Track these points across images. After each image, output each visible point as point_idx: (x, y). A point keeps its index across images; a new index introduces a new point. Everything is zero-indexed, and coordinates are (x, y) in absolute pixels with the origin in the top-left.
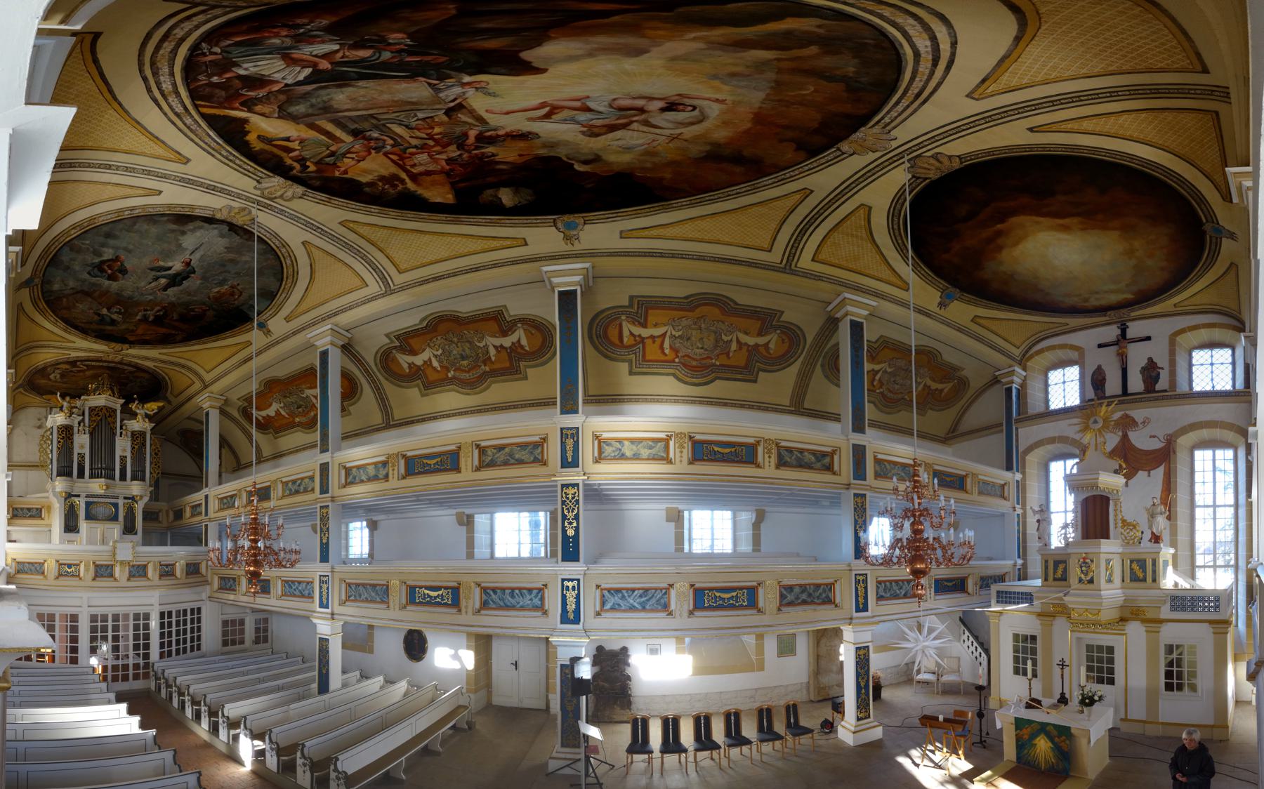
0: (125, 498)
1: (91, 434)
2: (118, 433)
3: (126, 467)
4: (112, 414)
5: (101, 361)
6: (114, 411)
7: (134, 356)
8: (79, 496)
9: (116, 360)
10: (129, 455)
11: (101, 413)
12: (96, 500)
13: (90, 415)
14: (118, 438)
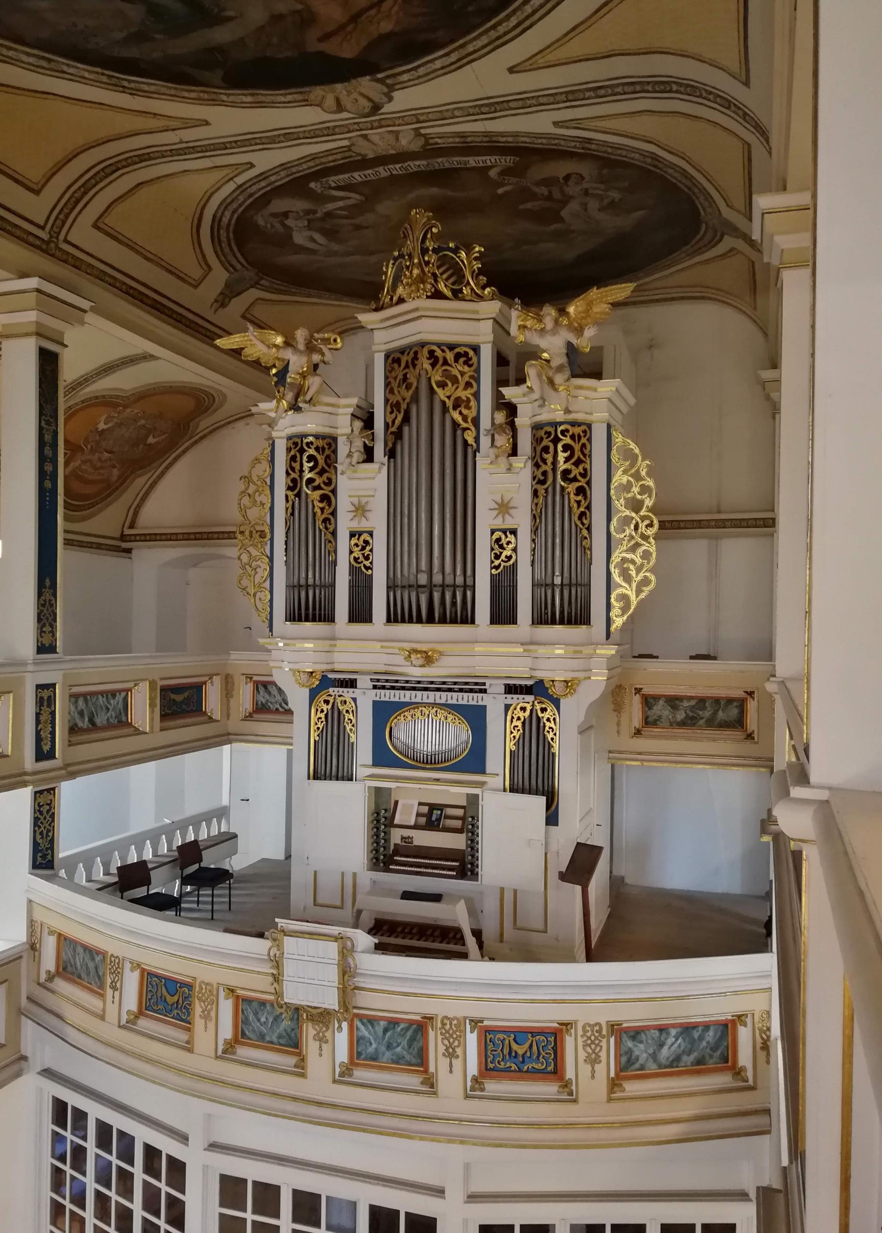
0: (510, 689)
1: (391, 454)
2: (485, 441)
5: (364, 163)
7: (446, 113)
8: (351, 684)
10: (522, 520)
12: (406, 696)
13: (387, 384)
14: (482, 462)
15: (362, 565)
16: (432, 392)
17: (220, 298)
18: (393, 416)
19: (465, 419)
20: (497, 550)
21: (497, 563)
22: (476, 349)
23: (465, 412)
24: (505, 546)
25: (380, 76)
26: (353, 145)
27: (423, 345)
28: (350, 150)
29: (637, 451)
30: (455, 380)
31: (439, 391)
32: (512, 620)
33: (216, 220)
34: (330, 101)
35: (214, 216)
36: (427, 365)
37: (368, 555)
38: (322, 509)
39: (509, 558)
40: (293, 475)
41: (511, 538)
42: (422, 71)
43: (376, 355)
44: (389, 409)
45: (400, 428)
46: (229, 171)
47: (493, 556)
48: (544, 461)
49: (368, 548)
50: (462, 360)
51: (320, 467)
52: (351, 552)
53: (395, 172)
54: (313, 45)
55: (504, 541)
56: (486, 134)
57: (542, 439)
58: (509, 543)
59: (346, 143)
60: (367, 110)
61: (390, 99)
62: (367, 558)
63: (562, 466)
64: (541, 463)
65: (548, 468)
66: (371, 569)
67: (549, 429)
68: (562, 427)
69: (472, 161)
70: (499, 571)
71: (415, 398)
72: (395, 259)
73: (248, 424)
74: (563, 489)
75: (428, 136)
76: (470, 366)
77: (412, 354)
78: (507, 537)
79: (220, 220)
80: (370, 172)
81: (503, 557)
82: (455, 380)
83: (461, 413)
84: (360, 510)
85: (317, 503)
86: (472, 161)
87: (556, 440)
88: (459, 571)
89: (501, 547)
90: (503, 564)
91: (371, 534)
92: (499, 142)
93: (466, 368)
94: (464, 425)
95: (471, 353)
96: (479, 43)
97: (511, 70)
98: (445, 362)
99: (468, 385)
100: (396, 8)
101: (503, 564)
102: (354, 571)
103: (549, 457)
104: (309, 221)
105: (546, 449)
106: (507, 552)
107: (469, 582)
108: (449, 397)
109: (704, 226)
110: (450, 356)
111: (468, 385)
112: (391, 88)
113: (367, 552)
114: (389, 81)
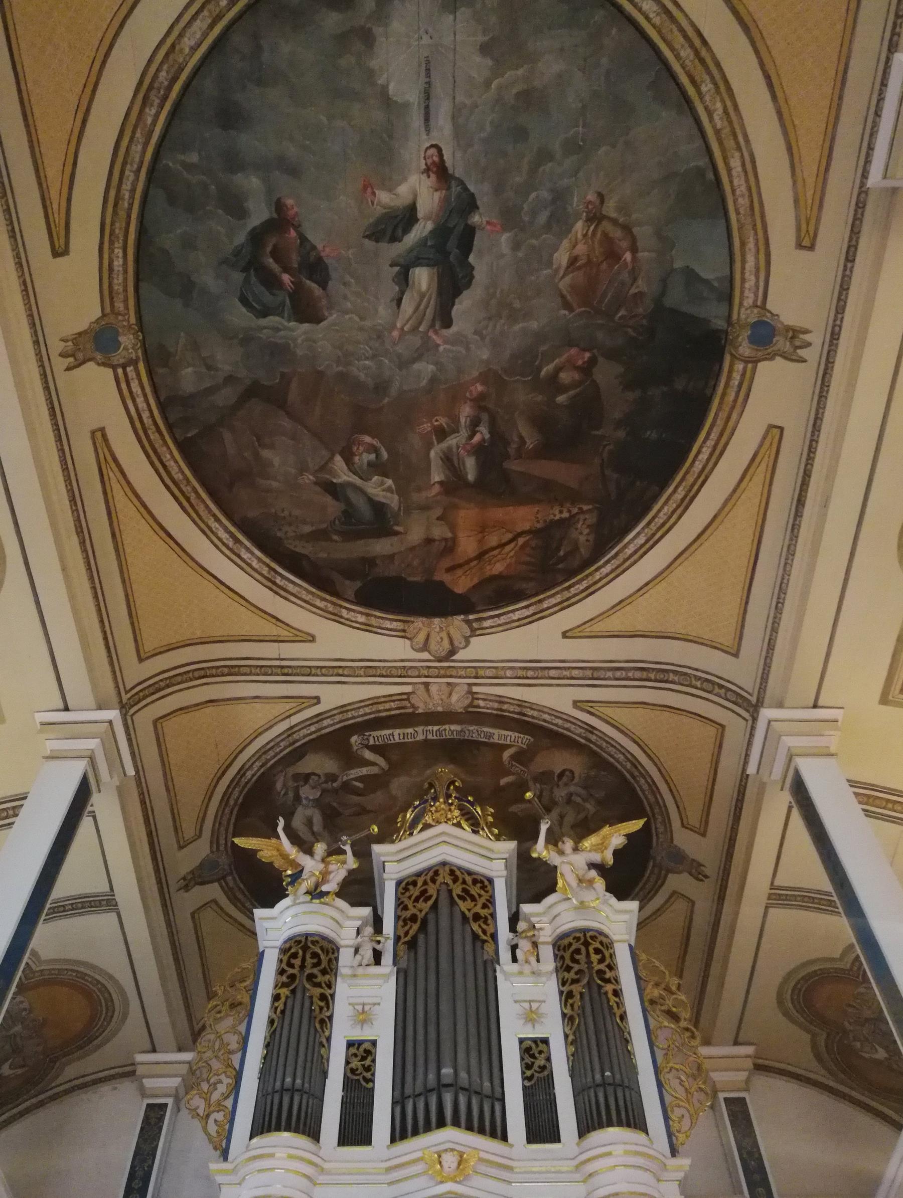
2: (505, 954)
3: (549, 1081)
4: (475, 890)
6: (485, 883)
9: (457, 701)
11: (432, 890)
15: (360, 1078)
16: (453, 903)
17: (189, 877)
18: (407, 928)
19: (484, 932)
20: (529, 1060)
21: (529, 1073)
22: (491, 881)
23: (484, 926)
24: (537, 1055)
25: (471, 617)
26: (413, 693)
27: (444, 864)
28: (408, 699)
29: (662, 968)
30: (473, 899)
31: (460, 902)
32: (555, 1137)
33: (242, 772)
34: (421, 637)
35: (243, 766)
36: (449, 880)
37: (370, 1066)
38: (321, 1008)
39: (543, 1068)
40: (291, 971)
41: (542, 1047)
42: (503, 619)
43: (387, 883)
44: (401, 923)
45: (415, 938)
46: (295, 705)
47: (524, 1066)
48: (577, 962)
49: (369, 1059)
50: (479, 885)
51: (323, 966)
52: (347, 1063)
53: (430, 737)
54: (441, 576)
55: (535, 1051)
56: (521, 703)
57: (570, 944)
58: (540, 1052)
59: (408, 689)
60: (443, 654)
61: (468, 643)
62: (368, 1069)
63: (597, 967)
64: (571, 964)
65: (583, 966)
66: (373, 1081)
67: (578, 935)
68: (591, 933)
69: (499, 735)
70: (533, 1082)
71: (435, 907)
72: (415, 808)
73: (115, 1089)
74: (600, 987)
75: (476, 696)
76: (487, 892)
77: (431, 874)
78: (537, 1046)
79: (244, 774)
80: (410, 730)
81: (536, 1067)
82: (473, 899)
83: (480, 926)
84: (363, 1016)
85: (315, 1000)
86: (499, 735)
87: (586, 944)
88: (486, 1076)
89: (533, 1056)
90: (536, 1075)
91: (374, 1043)
92: (525, 715)
93: (482, 892)
94: (485, 938)
95: (486, 883)
96: (553, 601)
97: (565, 635)
98: (464, 882)
99: (485, 906)
100: (512, 554)
101: (536, 1075)
102: (348, 1084)
103: (582, 958)
104: (324, 791)
105: (578, 951)
106: (541, 1061)
107: (498, 1094)
108: (469, 910)
109: (651, 864)
110: (469, 879)
111: (485, 906)
112: (474, 633)
113: (367, 1062)
114: (475, 625)
